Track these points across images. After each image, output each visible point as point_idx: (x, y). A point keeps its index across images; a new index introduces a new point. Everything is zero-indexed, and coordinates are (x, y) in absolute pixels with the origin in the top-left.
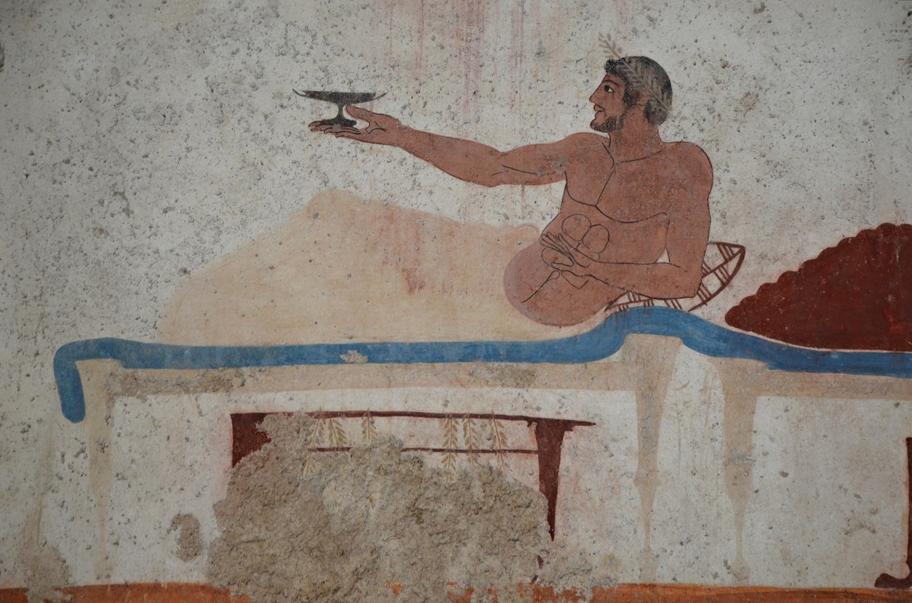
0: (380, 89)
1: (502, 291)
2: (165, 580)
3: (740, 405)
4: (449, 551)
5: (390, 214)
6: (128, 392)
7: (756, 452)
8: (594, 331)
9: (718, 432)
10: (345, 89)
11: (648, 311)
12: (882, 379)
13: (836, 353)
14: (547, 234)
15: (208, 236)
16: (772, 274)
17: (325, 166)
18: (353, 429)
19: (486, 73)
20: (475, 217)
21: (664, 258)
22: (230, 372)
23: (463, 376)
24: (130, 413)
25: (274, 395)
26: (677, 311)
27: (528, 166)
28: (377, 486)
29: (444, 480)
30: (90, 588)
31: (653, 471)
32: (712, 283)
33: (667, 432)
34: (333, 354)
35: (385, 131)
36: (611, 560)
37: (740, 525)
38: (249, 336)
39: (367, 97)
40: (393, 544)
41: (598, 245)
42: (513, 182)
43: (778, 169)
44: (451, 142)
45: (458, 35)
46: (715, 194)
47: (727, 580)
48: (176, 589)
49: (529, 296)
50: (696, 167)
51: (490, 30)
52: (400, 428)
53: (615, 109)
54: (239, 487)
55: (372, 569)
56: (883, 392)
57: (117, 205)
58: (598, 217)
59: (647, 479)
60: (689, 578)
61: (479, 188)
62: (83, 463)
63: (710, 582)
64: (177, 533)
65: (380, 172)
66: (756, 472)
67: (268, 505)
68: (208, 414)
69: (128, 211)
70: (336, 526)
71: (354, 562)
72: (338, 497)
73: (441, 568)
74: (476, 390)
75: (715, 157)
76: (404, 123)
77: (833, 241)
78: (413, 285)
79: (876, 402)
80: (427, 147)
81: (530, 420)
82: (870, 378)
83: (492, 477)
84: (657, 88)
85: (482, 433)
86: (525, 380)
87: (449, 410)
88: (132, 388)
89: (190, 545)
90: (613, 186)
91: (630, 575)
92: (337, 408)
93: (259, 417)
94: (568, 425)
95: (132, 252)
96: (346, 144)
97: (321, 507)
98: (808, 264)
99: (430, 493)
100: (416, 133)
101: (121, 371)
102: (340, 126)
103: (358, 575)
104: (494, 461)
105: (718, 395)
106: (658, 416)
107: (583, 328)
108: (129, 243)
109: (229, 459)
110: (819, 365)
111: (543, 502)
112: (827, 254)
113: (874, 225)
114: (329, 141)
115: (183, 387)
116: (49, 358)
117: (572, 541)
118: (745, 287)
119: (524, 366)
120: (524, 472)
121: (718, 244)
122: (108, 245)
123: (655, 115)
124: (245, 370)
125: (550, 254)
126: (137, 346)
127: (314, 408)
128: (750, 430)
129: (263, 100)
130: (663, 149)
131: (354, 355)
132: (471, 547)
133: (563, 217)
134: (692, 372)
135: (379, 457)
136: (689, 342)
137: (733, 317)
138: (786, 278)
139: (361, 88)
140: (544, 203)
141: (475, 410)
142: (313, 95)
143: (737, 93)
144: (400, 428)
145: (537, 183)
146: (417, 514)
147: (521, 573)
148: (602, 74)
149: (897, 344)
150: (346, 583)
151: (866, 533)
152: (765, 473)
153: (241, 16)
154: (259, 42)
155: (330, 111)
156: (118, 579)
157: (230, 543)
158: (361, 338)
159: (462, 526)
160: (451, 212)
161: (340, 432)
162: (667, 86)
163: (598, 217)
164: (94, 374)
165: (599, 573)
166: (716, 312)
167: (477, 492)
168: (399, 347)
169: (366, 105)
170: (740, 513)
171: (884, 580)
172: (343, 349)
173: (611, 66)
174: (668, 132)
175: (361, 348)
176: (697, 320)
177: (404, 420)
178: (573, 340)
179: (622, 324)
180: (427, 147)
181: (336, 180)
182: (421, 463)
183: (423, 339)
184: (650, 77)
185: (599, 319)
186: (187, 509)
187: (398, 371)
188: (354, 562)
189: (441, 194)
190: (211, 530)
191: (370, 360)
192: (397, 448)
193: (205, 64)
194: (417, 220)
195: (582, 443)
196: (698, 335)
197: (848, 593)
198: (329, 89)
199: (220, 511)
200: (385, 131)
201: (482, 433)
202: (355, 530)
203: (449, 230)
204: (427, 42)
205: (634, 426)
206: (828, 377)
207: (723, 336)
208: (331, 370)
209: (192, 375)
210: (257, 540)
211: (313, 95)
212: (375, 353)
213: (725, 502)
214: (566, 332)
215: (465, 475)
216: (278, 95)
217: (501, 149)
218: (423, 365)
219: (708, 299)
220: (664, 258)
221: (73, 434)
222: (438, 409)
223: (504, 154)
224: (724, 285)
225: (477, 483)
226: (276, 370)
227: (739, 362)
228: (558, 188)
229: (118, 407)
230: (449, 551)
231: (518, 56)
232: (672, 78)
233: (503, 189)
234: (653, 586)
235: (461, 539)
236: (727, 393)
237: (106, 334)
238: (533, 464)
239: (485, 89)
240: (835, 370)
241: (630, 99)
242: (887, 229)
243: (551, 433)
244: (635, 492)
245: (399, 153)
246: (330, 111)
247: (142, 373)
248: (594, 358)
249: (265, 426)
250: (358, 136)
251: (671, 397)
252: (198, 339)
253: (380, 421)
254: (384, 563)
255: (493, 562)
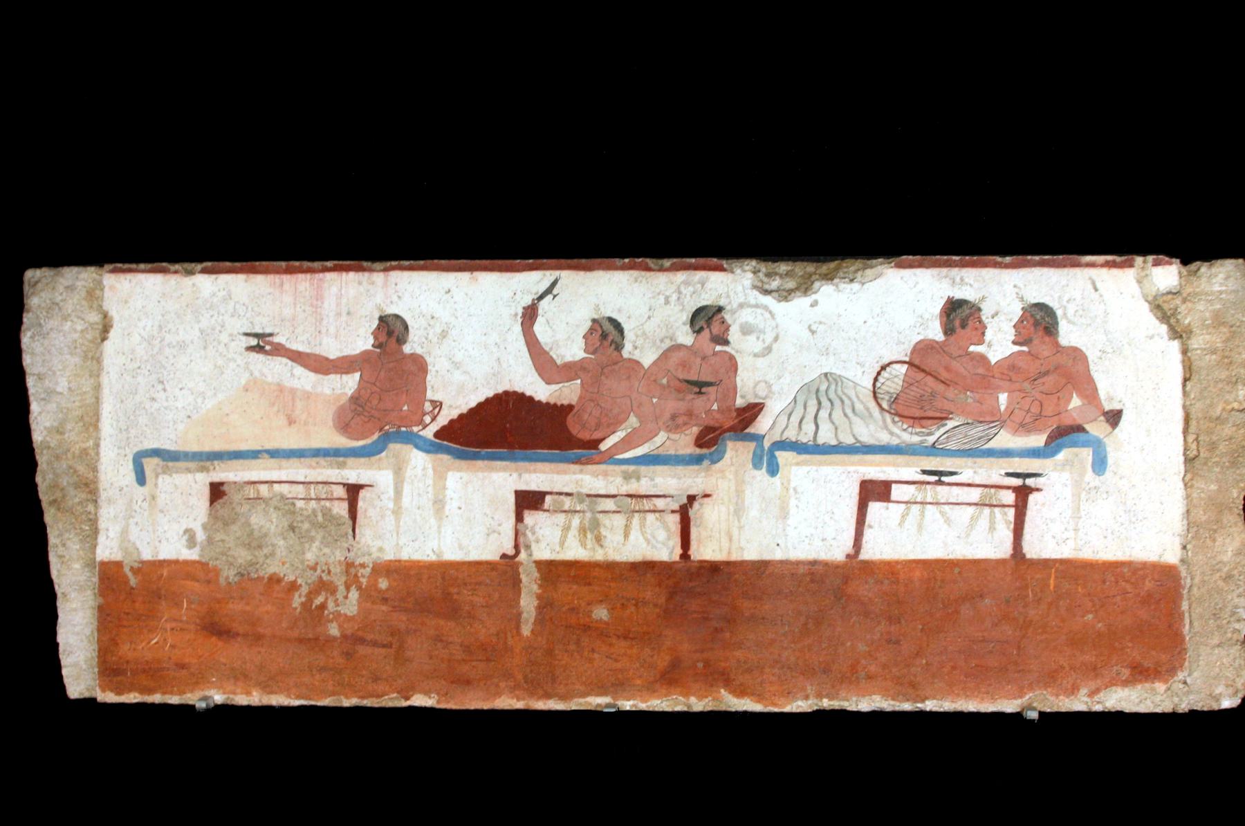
0: (276, 331)
1: (331, 423)
2: (182, 558)
3: (440, 476)
4: (307, 546)
5: (281, 388)
6: (164, 473)
7: (448, 498)
8: (373, 443)
9: (430, 489)
10: (260, 331)
11: (398, 432)
12: (504, 463)
13: (484, 451)
14: (352, 397)
15: (199, 400)
16: (454, 414)
17: (252, 367)
18: (264, 489)
19: (325, 322)
20: (319, 390)
21: (405, 408)
22: (208, 463)
23: (314, 464)
24: (165, 482)
25: (227, 473)
26: (412, 433)
27: (343, 365)
28: (274, 515)
29: (305, 513)
30: (149, 562)
31: (400, 508)
32: (427, 419)
33: (407, 489)
34: (254, 455)
35: (279, 350)
36: (381, 549)
37: (439, 532)
38: (218, 446)
39: (271, 335)
40: (282, 543)
41: (375, 402)
42: (336, 373)
43: (457, 365)
44: (308, 355)
45: (312, 305)
46: (429, 378)
47: (433, 558)
48: (186, 562)
49: (344, 426)
50: (419, 365)
51: (326, 305)
52: (285, 489)
53: (383, 338)
54: (213, 515)
55: (273, 554)
56: (504, 469)
57: (160, 387)
58: (375, 389)
59: (397, 512)
60: (417, 556)
61: (320, 376)
62: (145, 505)
63: (425, 558)
64: (186, 537)
65: (277, 369)
66: (447, 507)
67: (226, 524)
68: (199, 483)
69: (165, 390)
70: (256, 534)
71: (265, 551)
72: (257, 520)
73: (304, 553)
74: (319, 470)
75: (429, 360)
76: (288, 345)
77: (482, 399)
78: (291, 422)
79: (501, 474)
80: (298, 357)
81: (344, 485)
82: (499, 463)
83: (327, 513)
84: (402, 329)
85: (322, 491)
86: (342, 466)
87: (308, 480)
88: (166, 470)
89: (192, 542)
90: (382, 373)
91: (389, 556)
92: (256, 479)
93: (222, 484)
94: (361, 487)
95: (166, 408)
96: (261, 357)
97: (249, 525)
98: (471, 411)
99: (299, 519)
100: (293, 351)
101: (161, 463)
102: (258, 349)
103: (266, 557)
104: (328, 504)
105: (430, 471)
106: (402, 482)
107: (368, 441)
108: (165, 404)
109: (208, 504)
110: (475, 457)
111: (351, 523)
112: (480, 405)
113: (500, 390)
114: (254, 356)
115: (188, 470)
116: (130, 457)
117: (363, 540)
118: (443, 421)
119: (341, 459)
120: (341, 509)
121: (432, 402)
122: (156, 405)
123: (401, 340)
124: (216, 462)
125: (353, 407)
126: (168, 452)
127: (246, 479)
128: (445, 488)
129: (224, 338)
130: (405, 357)
131: (266, 456)
132: (317, 543)
133: (359, 390)
134: (418, 461)
135: (274, 502)
136: (417, 447)
137: (438, 435)
138: (461, 416)
139: (268, 331)
140: (350, 383)
141: (319, 480)
142: (247, 334)
143: (438, 330)
144: (285, 489)
145: (347, 373)
146: (292, 528)
147: (339, 555)
148: (377, 322)
149: (511, 446)
150: (261, 560)
151: (496, 535)
152: (451, 507)
153: (215, 300)
154: (223, 311)
155: (254, 342)
156: (161, 557)
157: (210, 541)
158: (268, 446)
159: (313, 533)
160: (308, 388)
161: (258, 491)
162: (406, 328)
163: (375, 389)
164: (150, 464)
165: (374, 556)
166: (429, 433)
167: (320, 518)
168: (284, 451)
169: (270, 339)
170: (439, 527)
171: (504, 556)
172: (259, 452)
173: (382, 319)
174: (407, 349)
175: (268, 452)
176: (421, 437)
177: (287, 485)
178: (364, 447)
179: (386, 439)
180: (298, 357)
181: (257, 374)
182: (294, 504)
183: (295, 446)
184: (398, 324)
185: (375, 437)
186: (191, 526)
187: (284, 462)
188: (265, 551)
189: (304, 379)
190: (201, 536)
191: (272, 457)
192: (283, 497)
193: (199, 322)
194: (293, 391)
195: (368, 495)
196: (421, 443)
197: (488, 563)
198: (253, 331)
199: (205, 527)
200: (279, 350)
201: (322, 491)
202: (266, 535)
203: (307, 396)
204: (298, 309)
205: (392, 487)
206: (480, 463)
207: (432, 444)
208: (254, 462)
209: (192, 465)
210: (223, 541)
211: (247, 334)
212: (274, 454)
213: (433, 521)
214: (361, 443)
215: (314, 511)
216: (231, 335)
217: (332, 357)
218: (295, 460)
219: (425, 427)
220: (405, 408)
221: (140, 492)
222: (302, 479)
223: (332, 361)
224: (433, 419)
225: (320, 515)
226: (229, 462)
227: (440, 456)
228: (357, 375)
229: (160, 479)
230: (307, 546)
231: (339, 314)
232: (409, 323)
233: (332, 376)
234: (399, 561)
235: (312, 539)
236: (434, 470)
237: (155, 445)
238: (345, 505)
239: (324, 330)
240: (483, 458)
241: (390, 333)
242: (506, 393)
243: (354, 491)
244: (392, 517)
245: (285, 360)
246: (254, 342)
247: (170, 464)
248: (373, 455)
249: (225, 488)
250: (267, 353)
251: (409, 473)
252: (194, 447)
253: (276, 486)
254: (278, 552)
255: (327, 550)
